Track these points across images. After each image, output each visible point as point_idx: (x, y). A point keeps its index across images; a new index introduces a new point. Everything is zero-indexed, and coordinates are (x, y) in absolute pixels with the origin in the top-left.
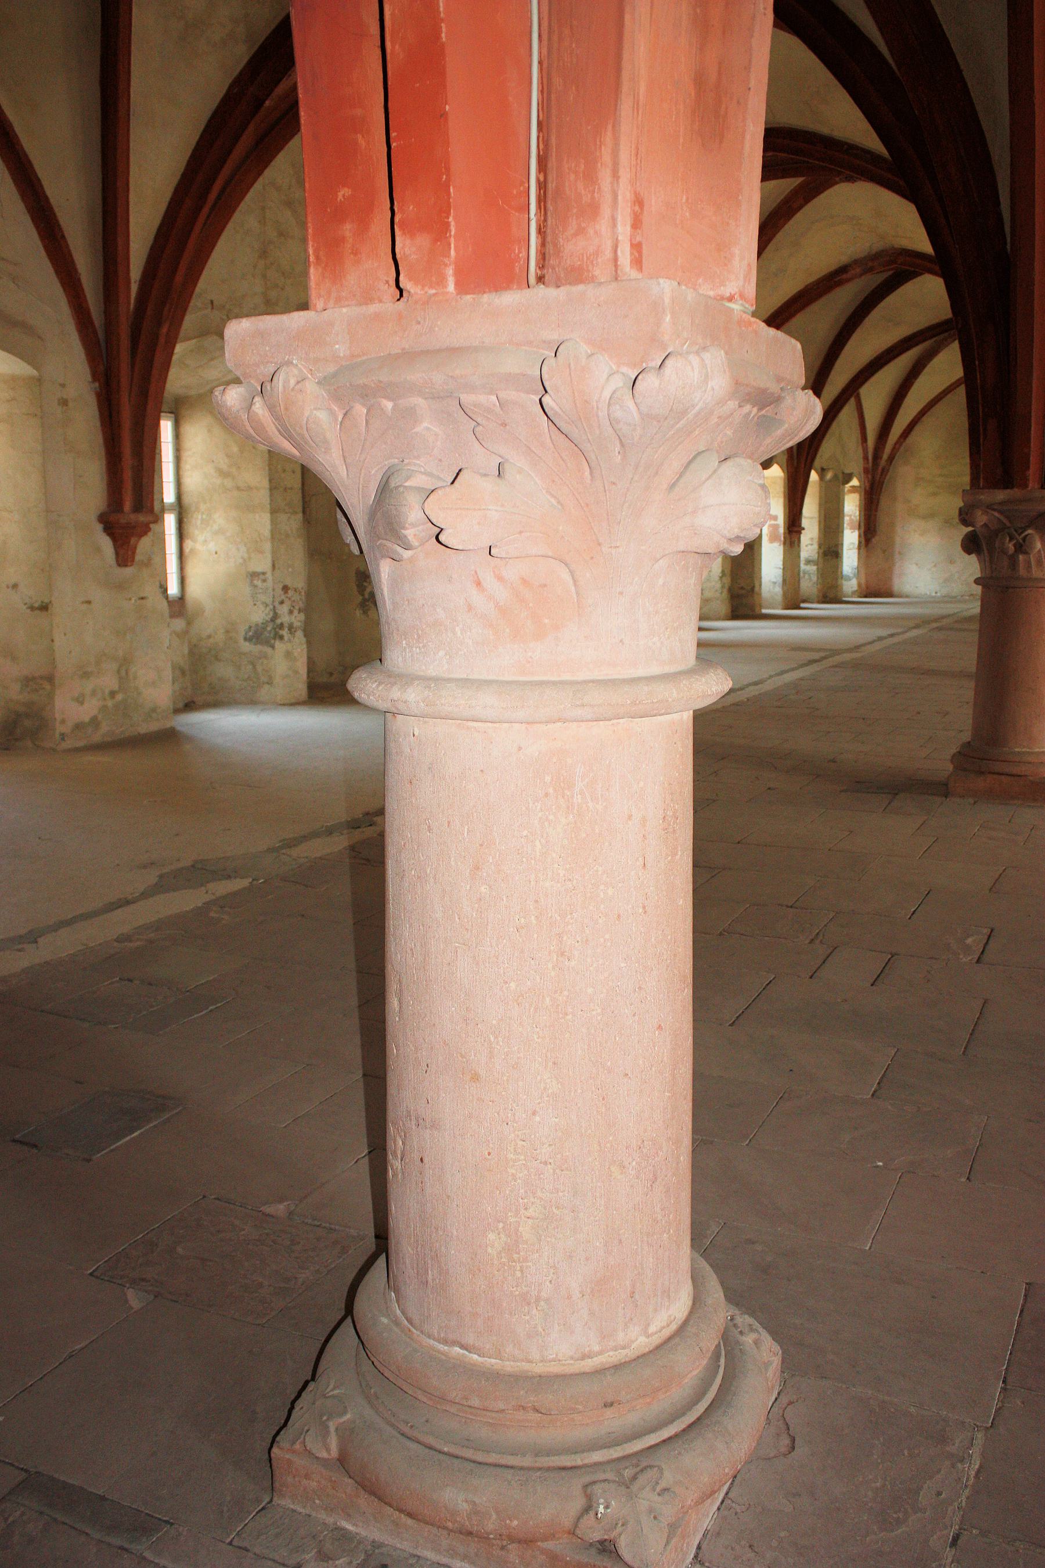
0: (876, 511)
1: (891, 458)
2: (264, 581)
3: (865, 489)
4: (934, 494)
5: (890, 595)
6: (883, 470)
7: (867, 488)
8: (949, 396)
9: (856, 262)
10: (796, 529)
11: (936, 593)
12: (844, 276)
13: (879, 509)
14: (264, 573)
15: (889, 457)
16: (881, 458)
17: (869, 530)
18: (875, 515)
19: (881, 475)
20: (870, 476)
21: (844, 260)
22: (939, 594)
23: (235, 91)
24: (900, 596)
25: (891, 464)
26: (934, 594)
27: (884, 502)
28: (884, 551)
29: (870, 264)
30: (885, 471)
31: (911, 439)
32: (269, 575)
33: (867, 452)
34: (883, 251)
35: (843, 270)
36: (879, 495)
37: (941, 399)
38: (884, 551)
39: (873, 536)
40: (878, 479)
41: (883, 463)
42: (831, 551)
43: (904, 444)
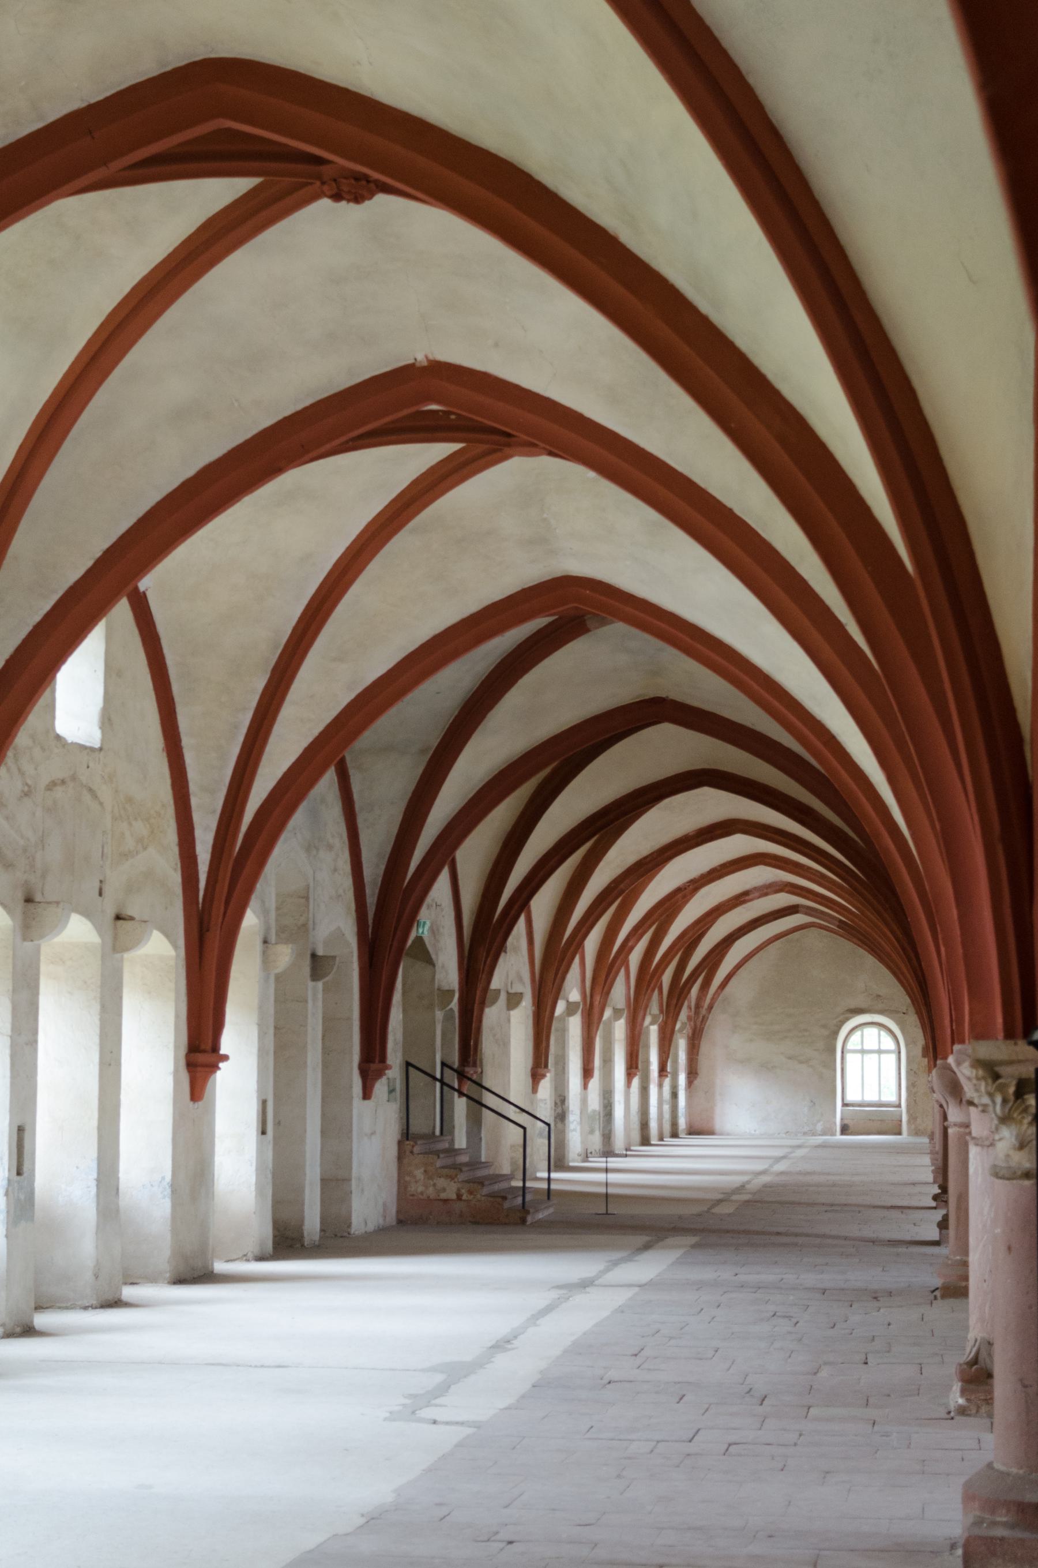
0: (697, 1054)
1: (710, 1008)
2: (546, 1104)
3: (688, 1036)
4: (751, 1040)
5: (710, 1132)
6: (704, 1017)
7: (690, 1035)
8: (762, 952)
9: (755, 888)
10: (665, 1073)
11: (755, 1131)
12: (747, 898)
13: (700, 1053)
14: (545, 1100)
15: (708, 1007)
16: (702, 1007)
17: (692, 1073)
18: (697, 1059)
19: (701, 1025)
20: (692, 1023)
21: (748, 887)
22: (757, 1132)
23: (612, 886)
24: (728, 1134)
25: (710, 1012)
26: (753, 1132)
27: (705, 1047)
28: (706, 1093)
29: (765, 891)
30: (704, 1020)
31: (728, 989)
32: (548, 1102)
33: (691, 1002)
34: (774, 882)
35: (746, 893)
36: (700, 1040)
37: (755, 954)
38: (706, 1093)
39: (695, 1078)
40: (698, 1026)
41: (703, 1011)
42: (674, 1095)
43: (721, 996)
